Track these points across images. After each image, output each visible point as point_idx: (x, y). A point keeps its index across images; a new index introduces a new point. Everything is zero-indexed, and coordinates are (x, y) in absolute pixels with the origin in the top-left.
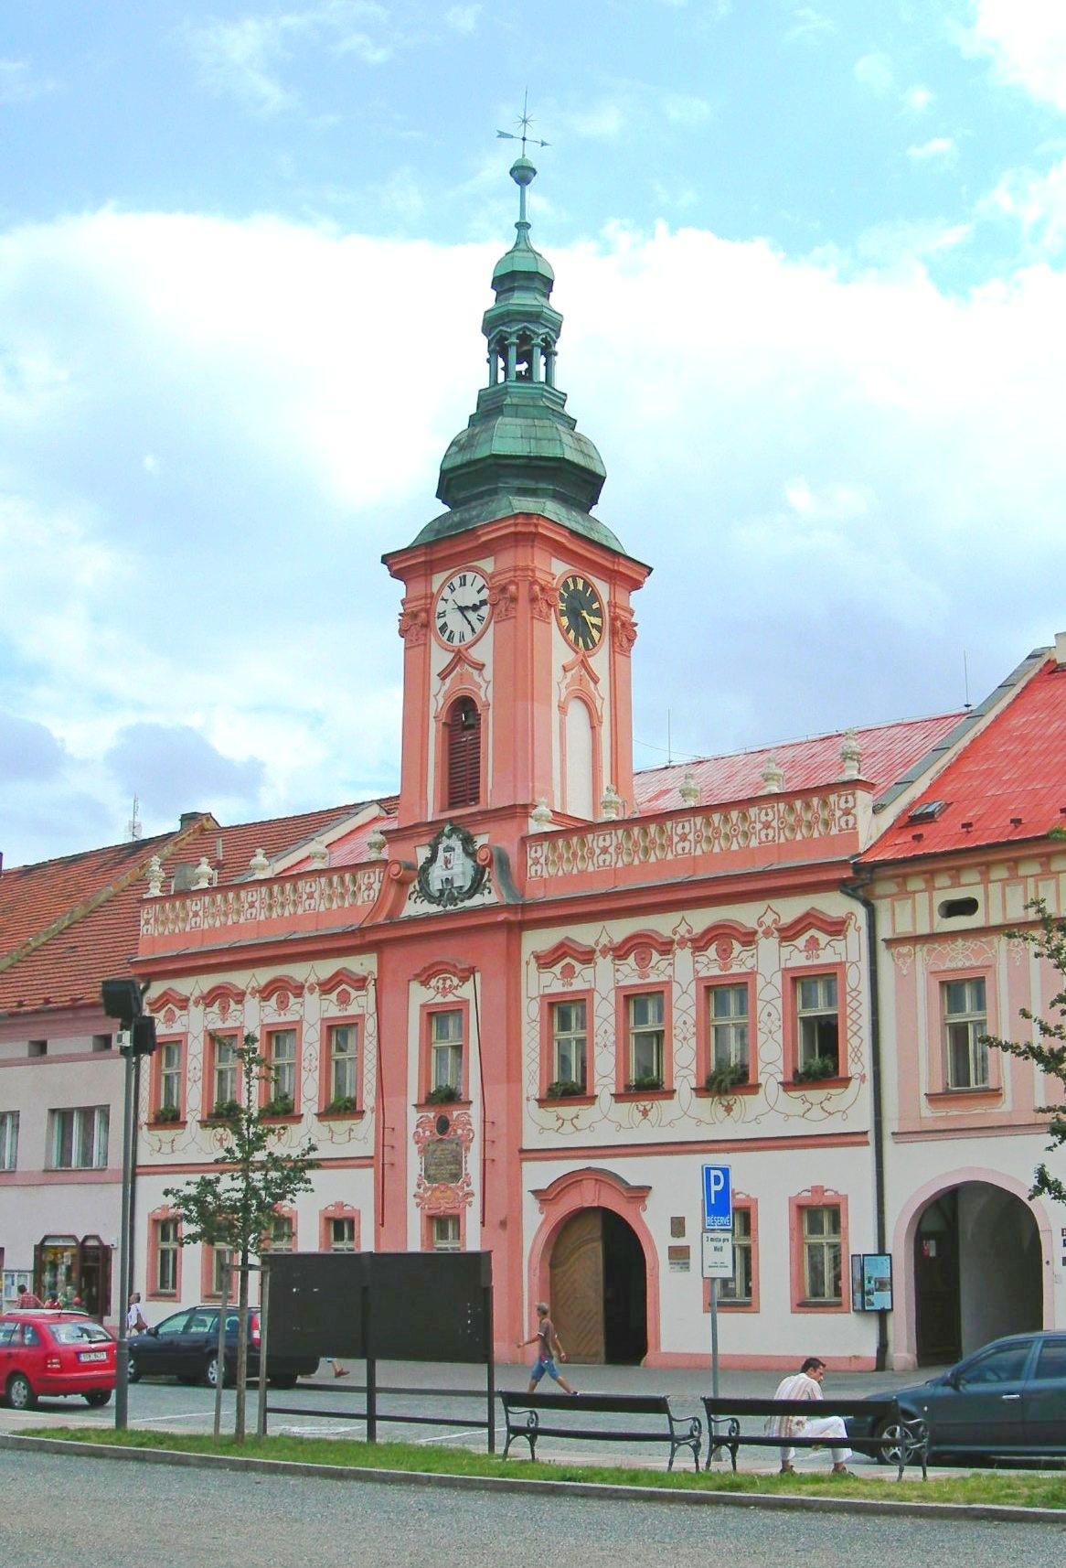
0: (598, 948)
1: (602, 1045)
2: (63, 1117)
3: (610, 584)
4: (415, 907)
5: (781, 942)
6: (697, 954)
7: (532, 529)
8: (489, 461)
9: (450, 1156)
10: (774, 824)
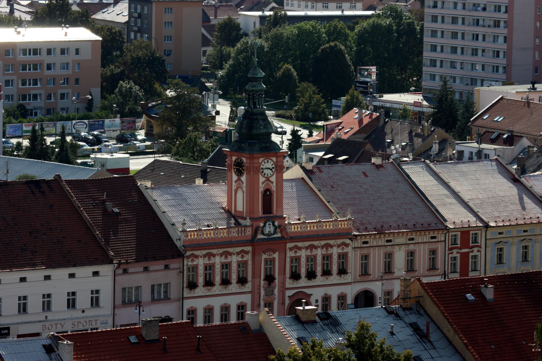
4: (260, 236)
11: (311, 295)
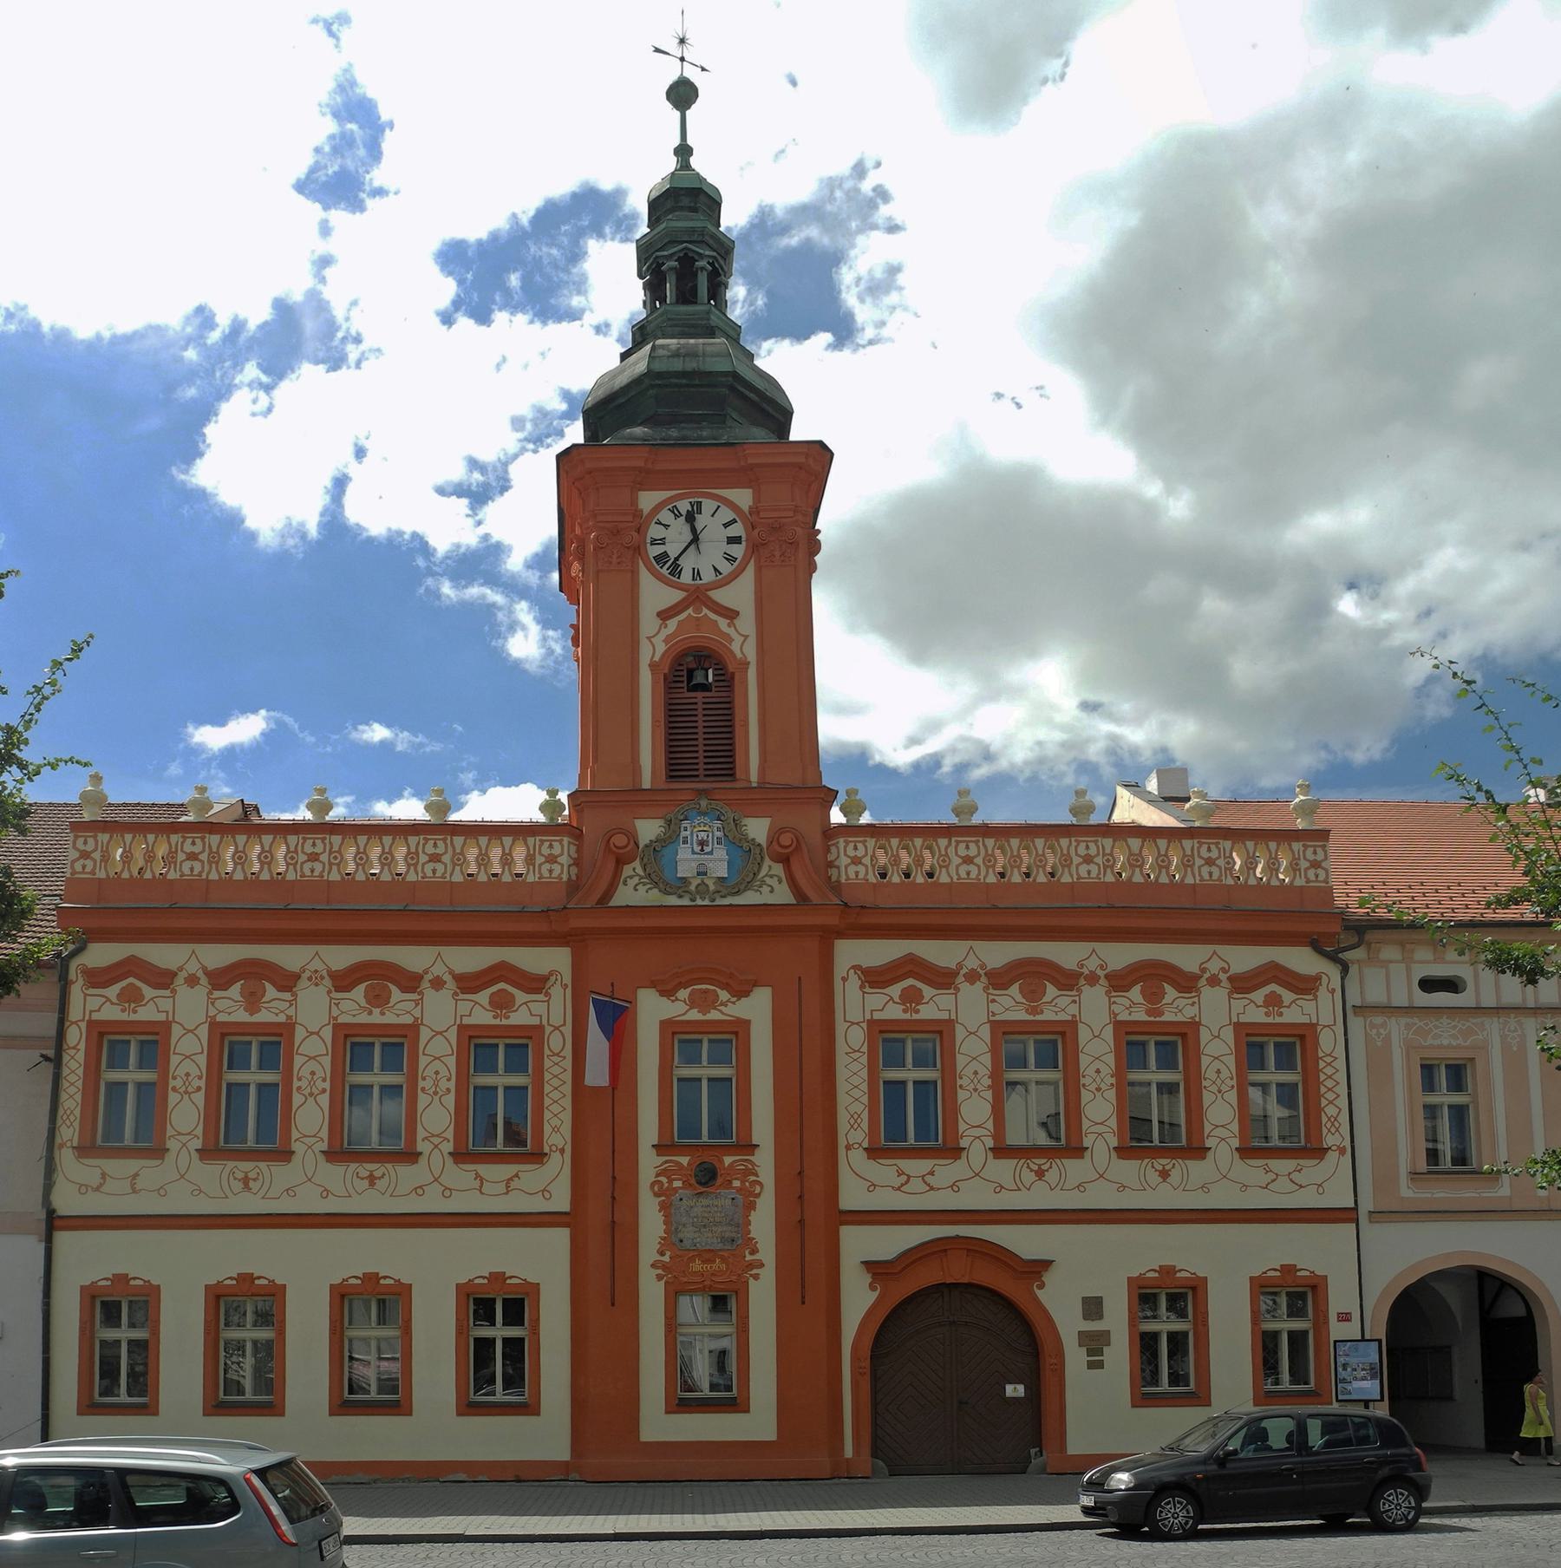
4: (633, 892)
6: (1114, 994)
11: (1046, 1264)
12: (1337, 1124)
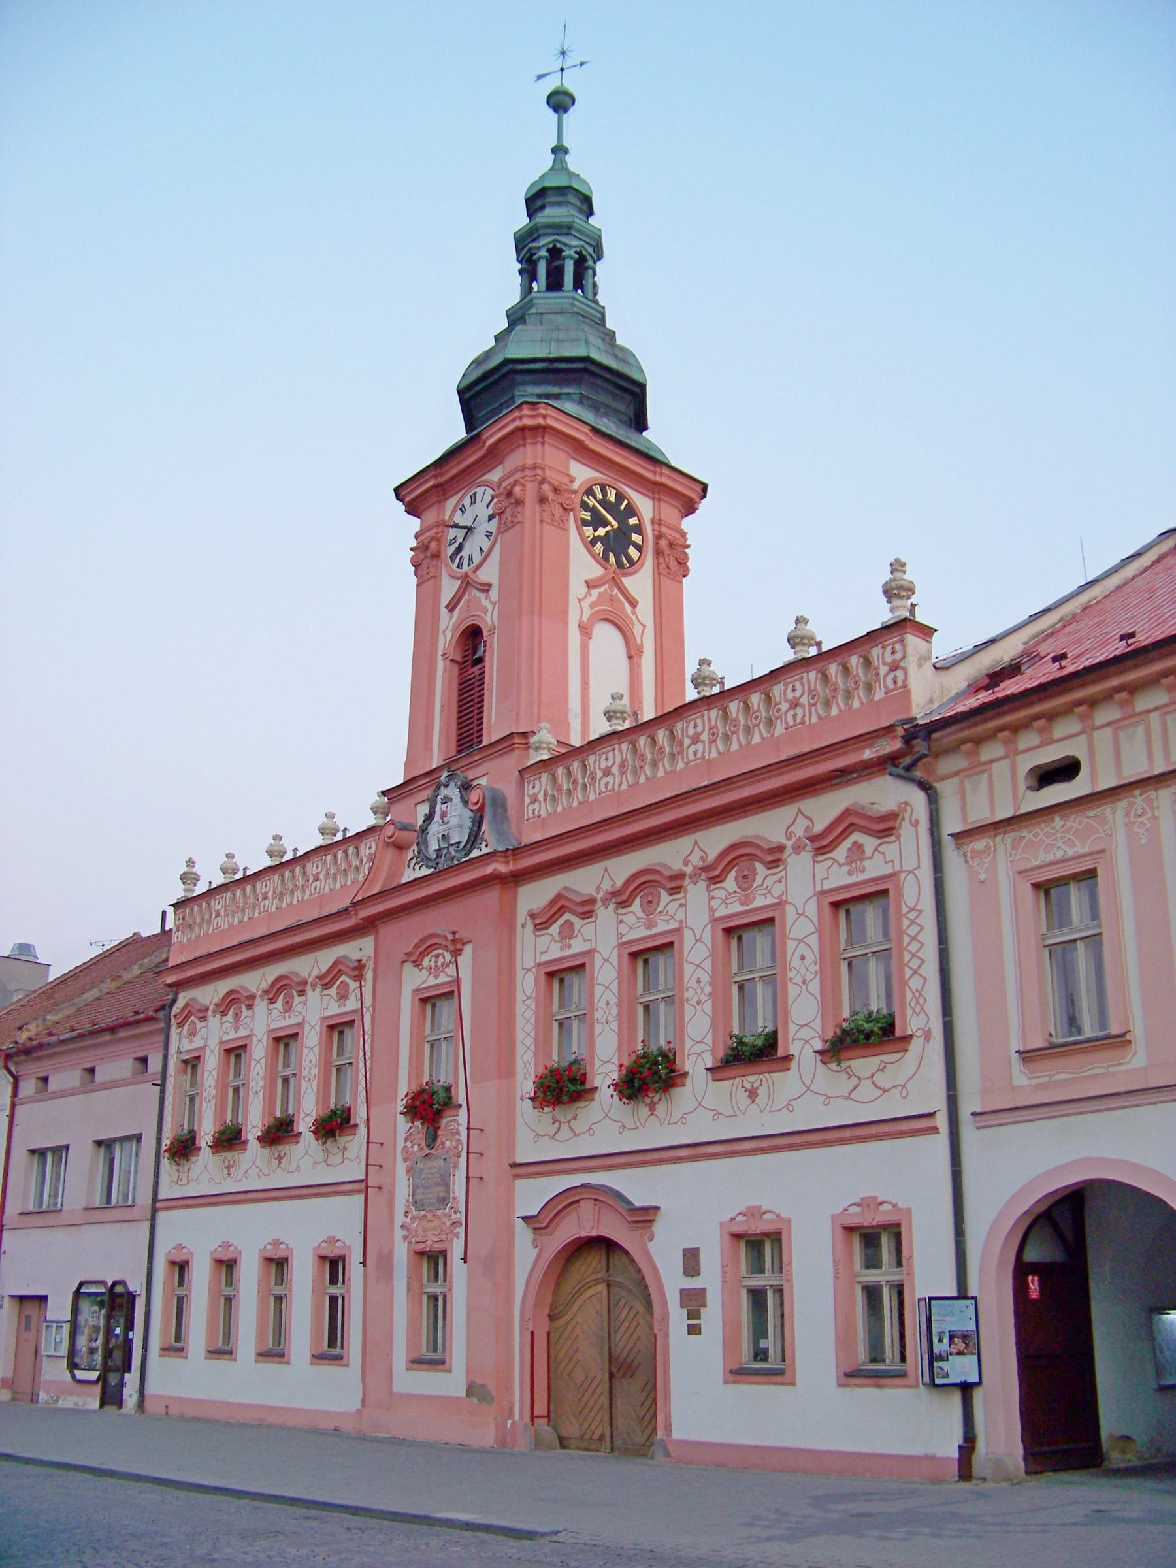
0: (599, 896)
1: (603, 1021)
2: (104, 1145)
3: (653, 499)
5: (815, 856)
6: (713, 887)
7: (541, 421)
8: (506, 369)
9: (437, 1175)
10: (804, 700)
12: (921, 1001)
